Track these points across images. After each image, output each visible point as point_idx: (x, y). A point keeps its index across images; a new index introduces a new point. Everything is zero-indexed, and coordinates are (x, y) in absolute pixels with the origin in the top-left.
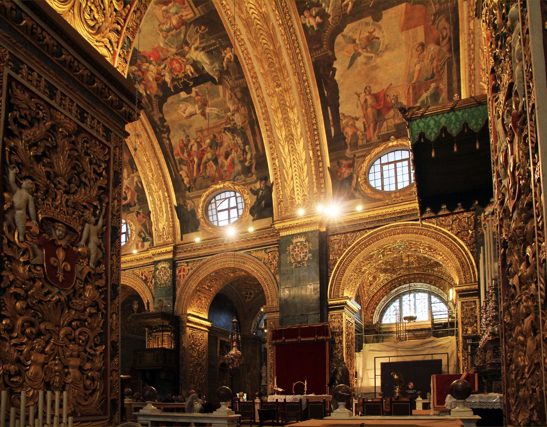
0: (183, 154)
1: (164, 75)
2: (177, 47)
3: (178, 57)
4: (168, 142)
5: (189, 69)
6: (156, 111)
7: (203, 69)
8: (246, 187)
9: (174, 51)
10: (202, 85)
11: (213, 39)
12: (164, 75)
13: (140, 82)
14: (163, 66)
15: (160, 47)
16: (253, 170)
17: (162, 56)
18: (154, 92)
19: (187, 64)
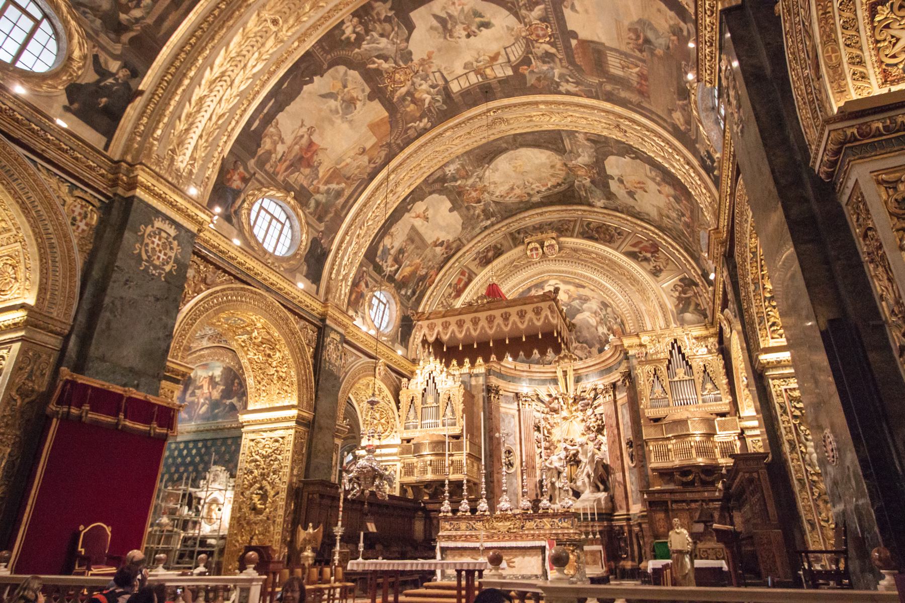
8: (91, 44)
16: (126, 37)
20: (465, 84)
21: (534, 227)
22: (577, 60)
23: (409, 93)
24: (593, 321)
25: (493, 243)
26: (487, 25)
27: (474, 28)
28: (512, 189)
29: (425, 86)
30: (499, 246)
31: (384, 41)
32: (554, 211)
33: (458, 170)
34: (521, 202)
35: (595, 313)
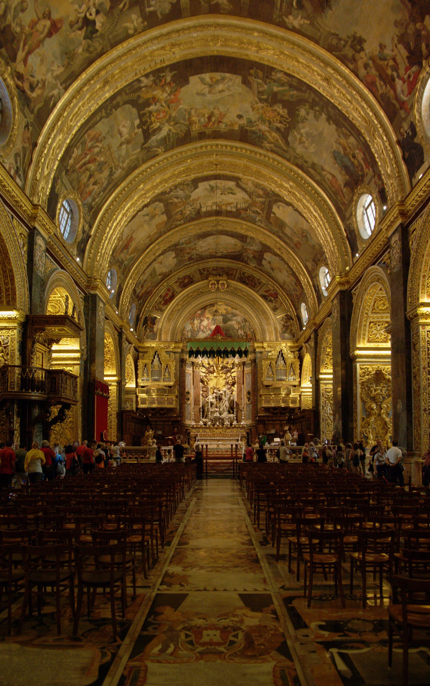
0: (90, 141)
1: (156, 105)
2: (175, 117)
3: (167, 117)
4: (98, 118)
5: (156, 125)
6: (125, 98)
7: (154, 135)
9: (173, 115)
10: (142, 136)
11: (174, 140)
12: (156, 105)
13: (154, 82)
14: (164, 104)
15: (180, 105)
17: (172, 105)
18: (142, 95)
19: (161, 124)
20: (209, 209)
21: (213, 268)
22: (271, 220)
23: (181, 211)
24: (236, 327)
25: (188, 274)
26: (232, 194)
27: (226, 193)
28: (209, 249)
29: (190, 208)
30: (192, 276)
31: (181, 191)
32: (226, 262)
33: (186, 241)
34: (210, 255)
35: (239, 323)
